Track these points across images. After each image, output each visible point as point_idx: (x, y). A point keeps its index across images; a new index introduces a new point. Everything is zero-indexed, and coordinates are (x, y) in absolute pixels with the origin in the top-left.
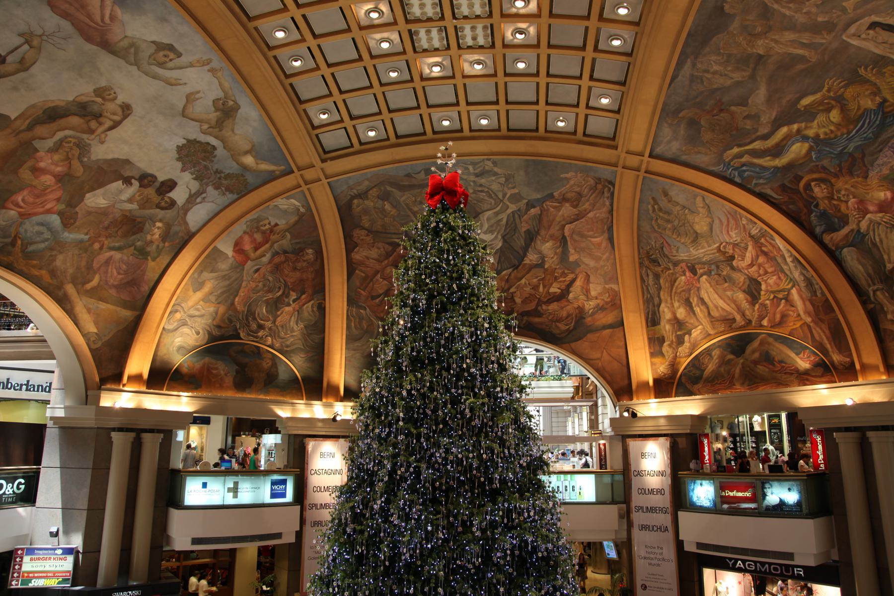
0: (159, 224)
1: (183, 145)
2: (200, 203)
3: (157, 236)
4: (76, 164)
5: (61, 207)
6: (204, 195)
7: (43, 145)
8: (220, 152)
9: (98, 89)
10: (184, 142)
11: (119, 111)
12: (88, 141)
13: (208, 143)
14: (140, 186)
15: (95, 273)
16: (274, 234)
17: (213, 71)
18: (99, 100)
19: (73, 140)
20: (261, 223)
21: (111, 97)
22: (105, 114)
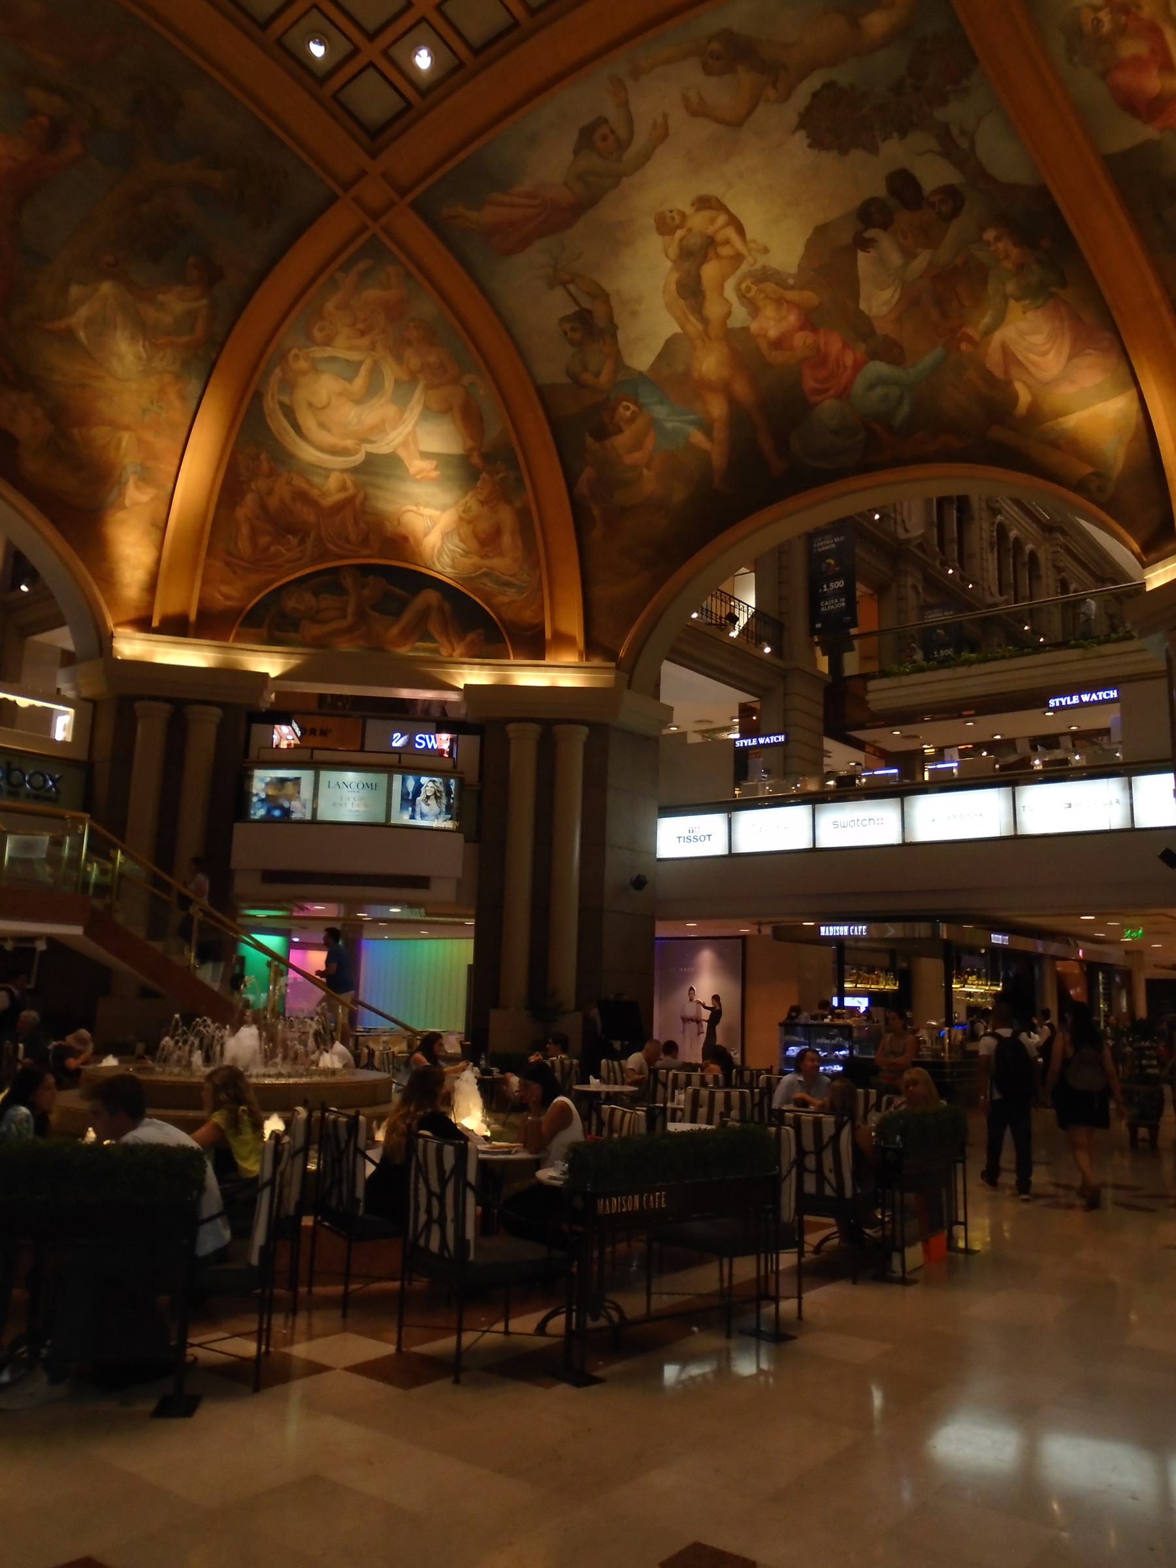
0: (990, 235)
1: (808, 137)
2: (972, 143)
3: (1015, 252)
4: (791, 295)
5: (862, 347)
6: (955, 131)
7: (740, 316)
8: (843, 76)
9: (658, 229)
10: (801, 135)
11: (707, 214)
12: (758, 266)
13: (815, 95)
14: (885, 226)
15: (1009, 383)
16: (1139, 7)
17: (636, 74)
18: (680, 233)
19: (748, 282)
20: (1088, 27)
21: (676, 217)
22: (711, 230)
